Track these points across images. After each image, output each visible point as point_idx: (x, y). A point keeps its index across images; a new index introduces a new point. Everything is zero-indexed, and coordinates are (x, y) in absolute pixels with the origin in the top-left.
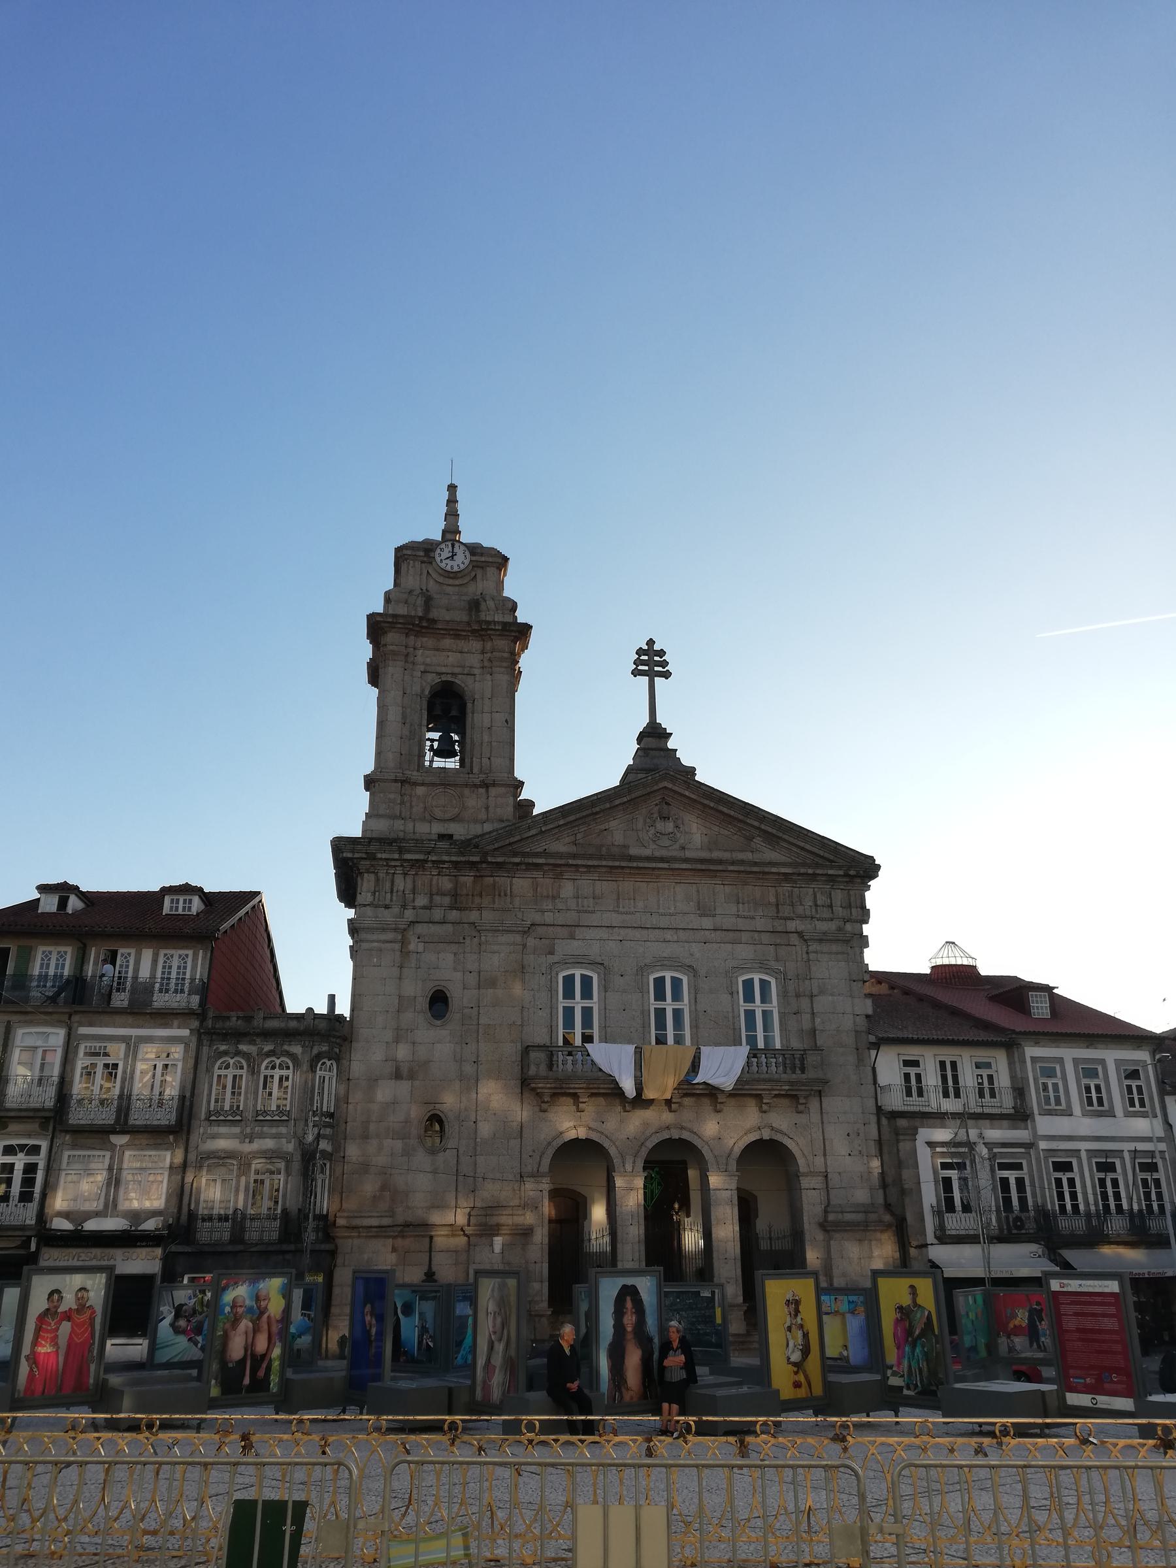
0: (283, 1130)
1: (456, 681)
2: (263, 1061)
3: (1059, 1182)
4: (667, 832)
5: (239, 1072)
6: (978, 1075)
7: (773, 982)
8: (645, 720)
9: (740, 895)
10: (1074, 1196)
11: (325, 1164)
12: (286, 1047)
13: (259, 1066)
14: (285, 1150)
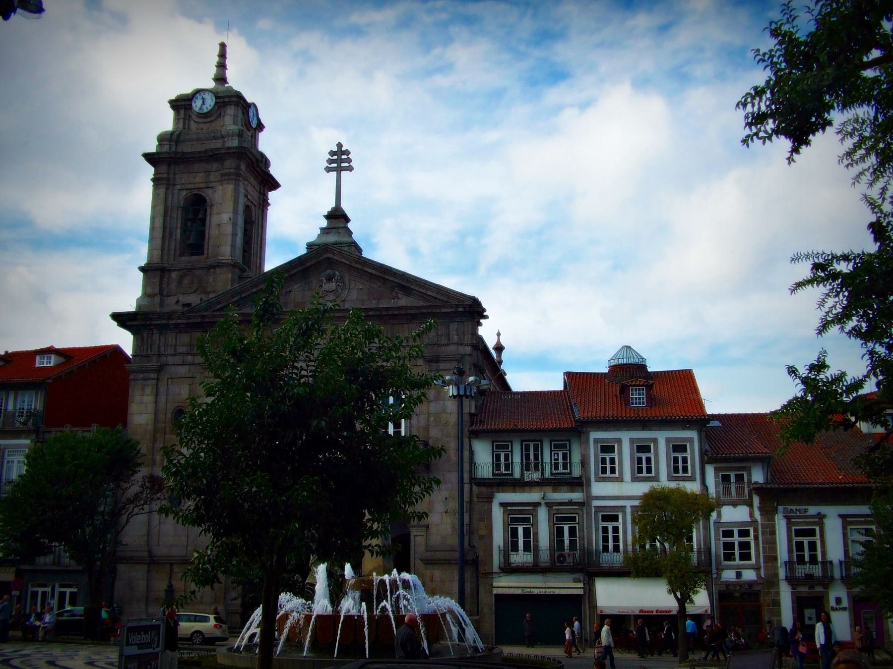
1: (201, 193)
4: (330, 290)
6: (555, 454)
8: (332, 204)
10: (616, 539)
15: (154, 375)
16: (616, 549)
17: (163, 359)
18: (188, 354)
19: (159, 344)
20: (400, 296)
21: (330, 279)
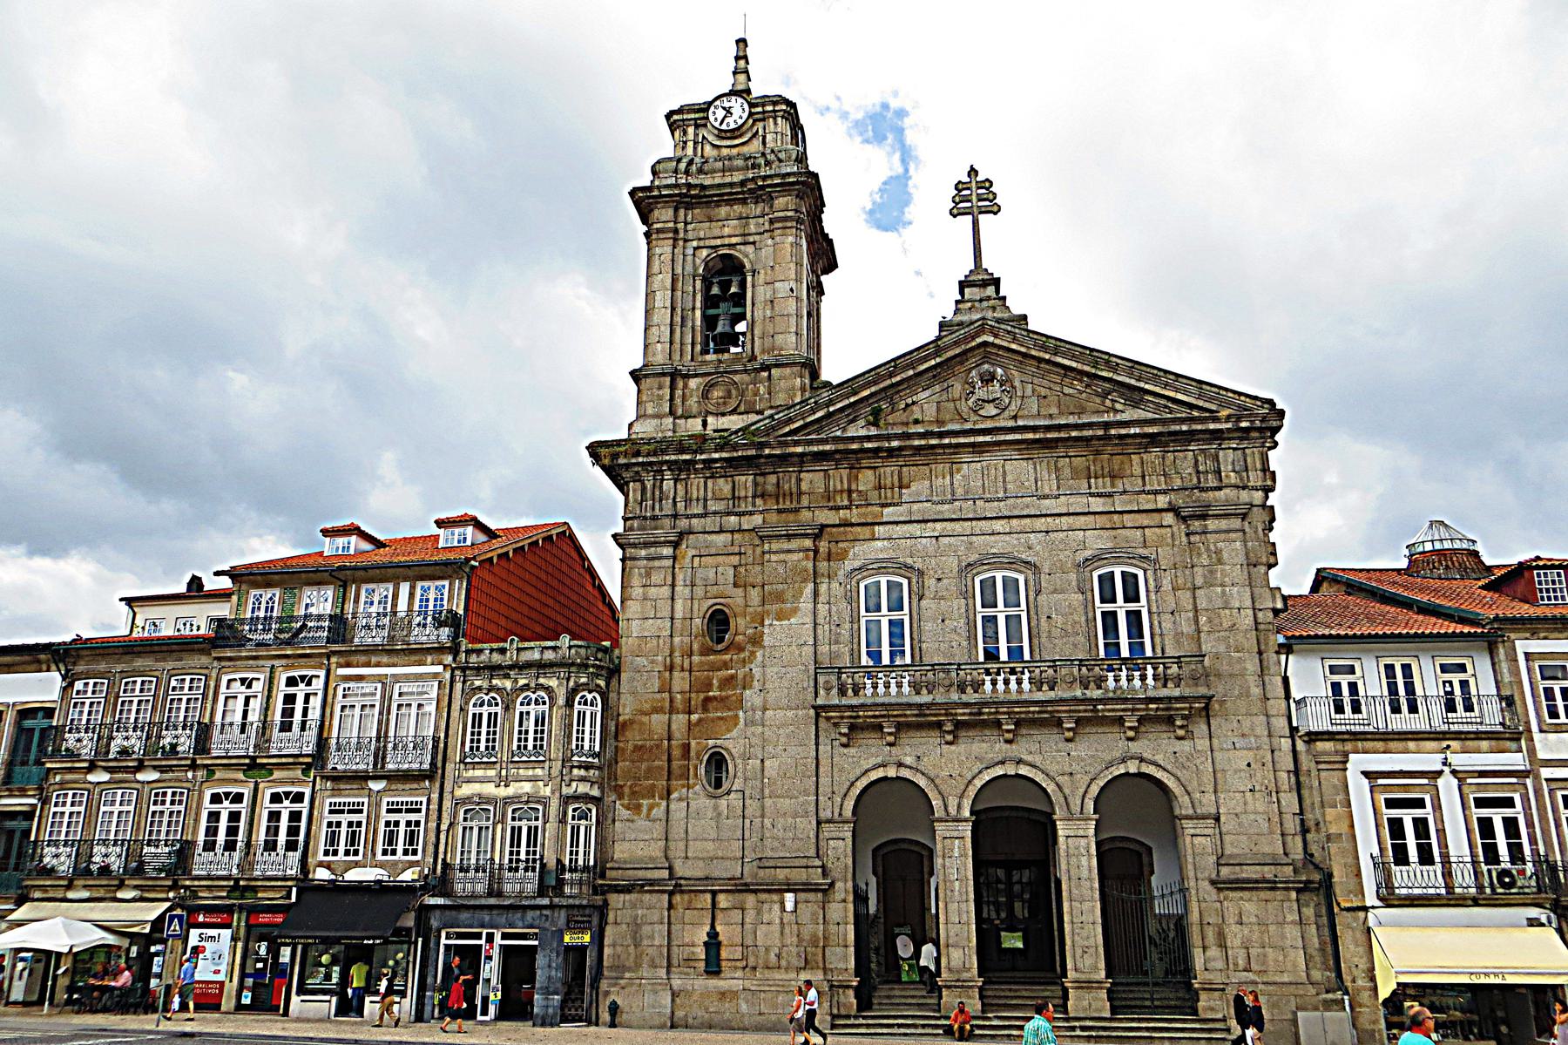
0: (539, 772)
2: (518, 696)
5: (493, 709)
6: (1444, 682)
7: (1140, 574)
9: (1092, 468)
11: (590, 810)
12: (542, 681)
13: (514, 702)
14: (542, 793)
15: (667, 551)
17: (683, 524)
18: (729, 514)
19: (674, 498)
21: (988, 379)
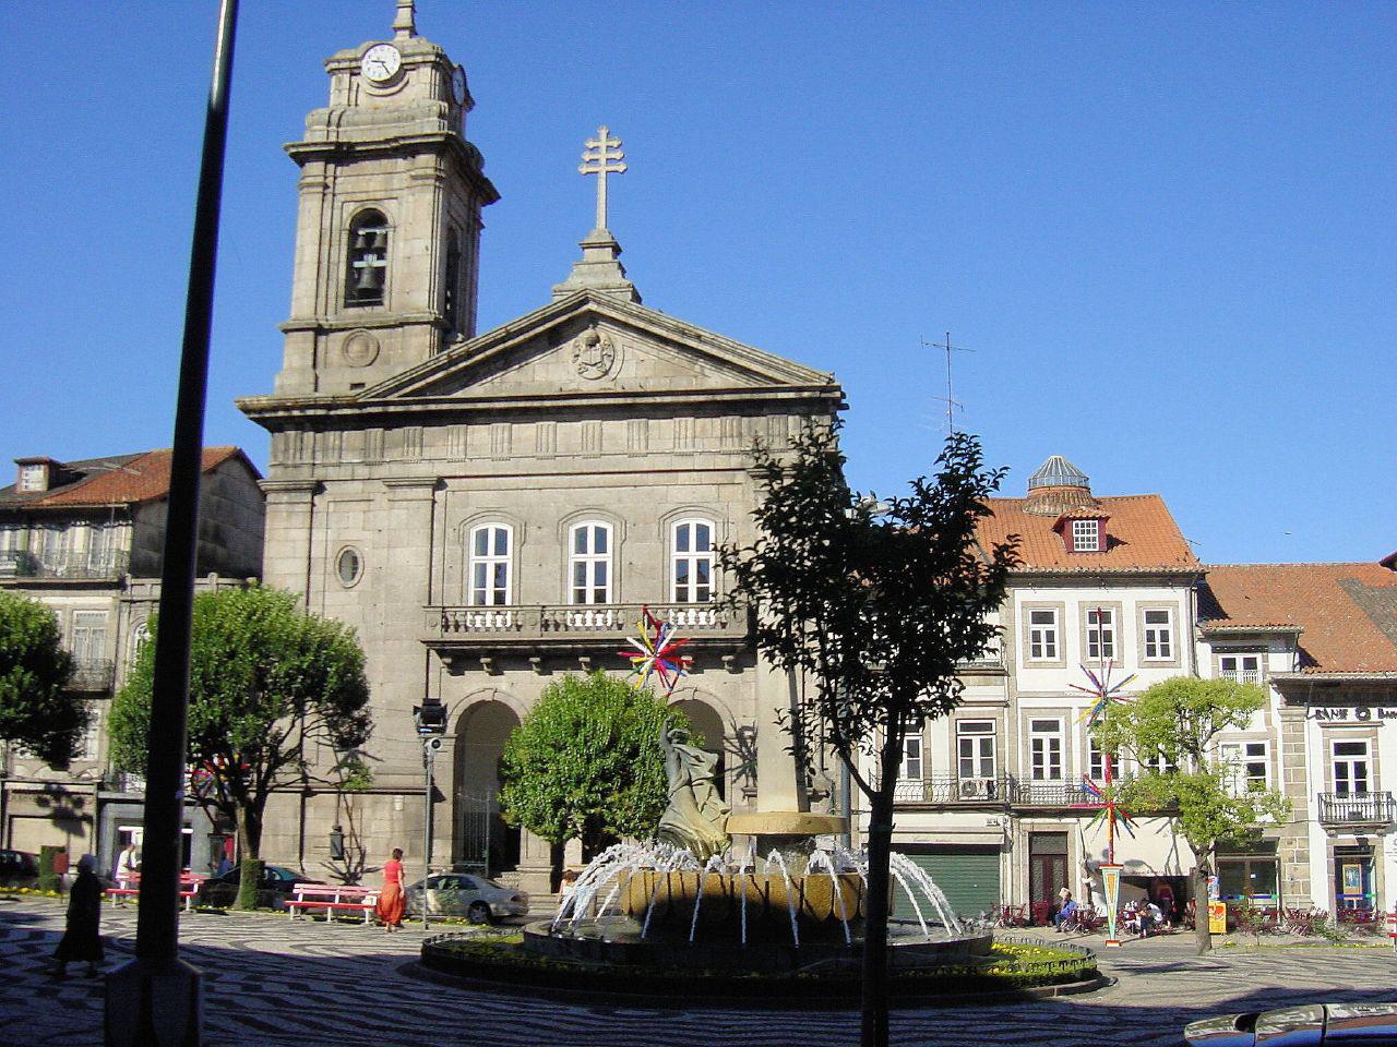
1: (379, 208)
3: (1038, 744)
4: (593, 363)
10: (1055, 759)
16: (1055, 773)
20: (707, 372)
